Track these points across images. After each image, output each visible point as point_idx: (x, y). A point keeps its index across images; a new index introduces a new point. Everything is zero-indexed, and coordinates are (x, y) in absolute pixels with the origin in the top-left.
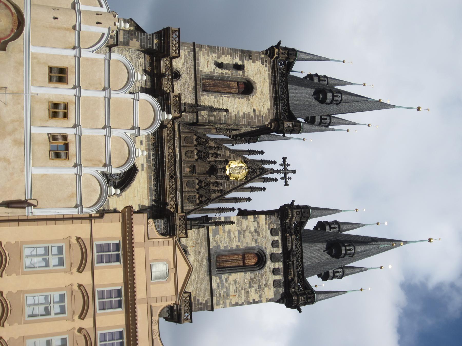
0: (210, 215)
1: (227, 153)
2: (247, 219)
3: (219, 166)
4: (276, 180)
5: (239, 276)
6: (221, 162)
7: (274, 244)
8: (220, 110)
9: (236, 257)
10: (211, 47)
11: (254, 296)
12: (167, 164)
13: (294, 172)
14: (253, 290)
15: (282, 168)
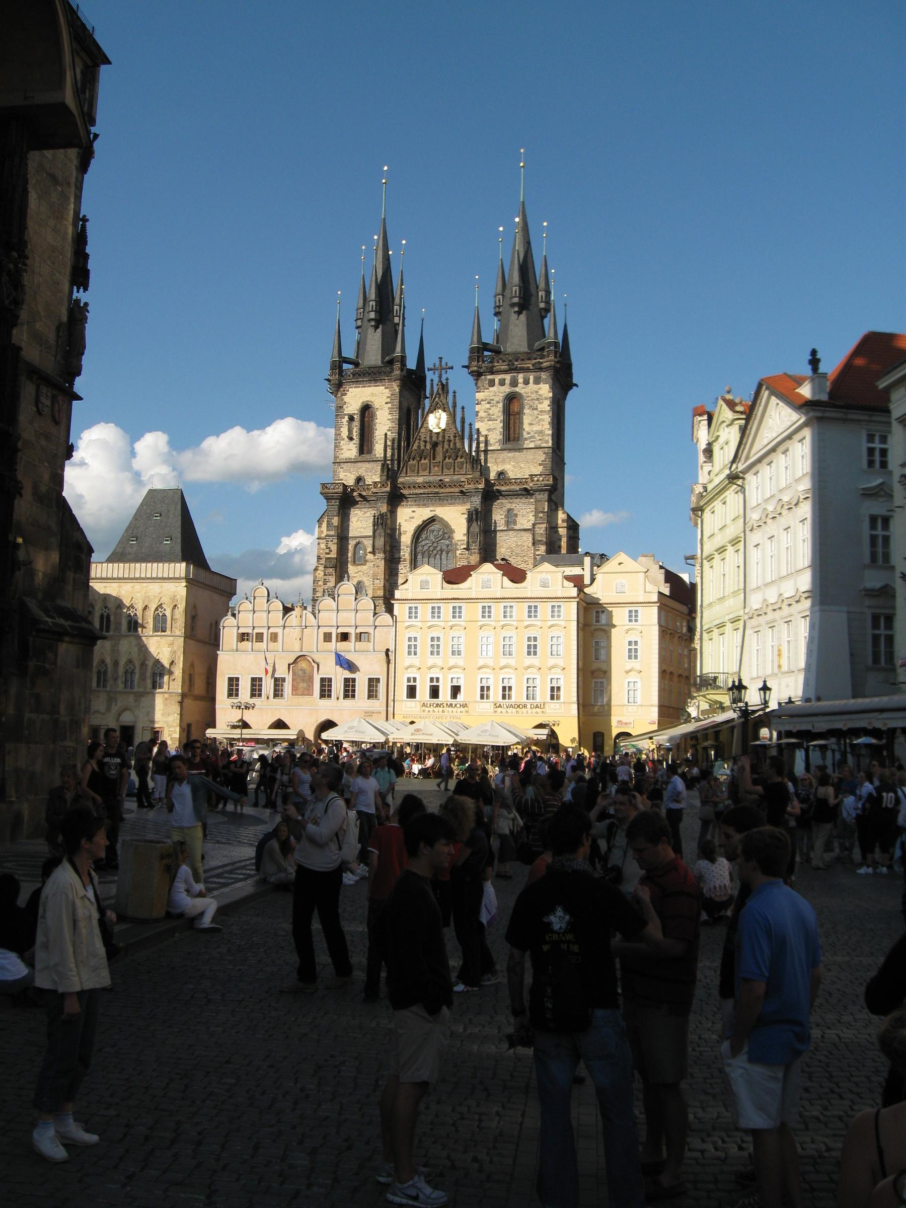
0: (474, 449)
1: (423, 430)
2: (478, 412)
3: (434, 439)
4: (447, 379)
5: (526, 420)
6: (431, 437)
7: (502, 383)
8: (386, 442)
9: (511, 422)
10: (336, 447)
11: (546, 405)
12: (429, 490)
13: (441, 358)
14: (540, 407)
15: (437, 372)
